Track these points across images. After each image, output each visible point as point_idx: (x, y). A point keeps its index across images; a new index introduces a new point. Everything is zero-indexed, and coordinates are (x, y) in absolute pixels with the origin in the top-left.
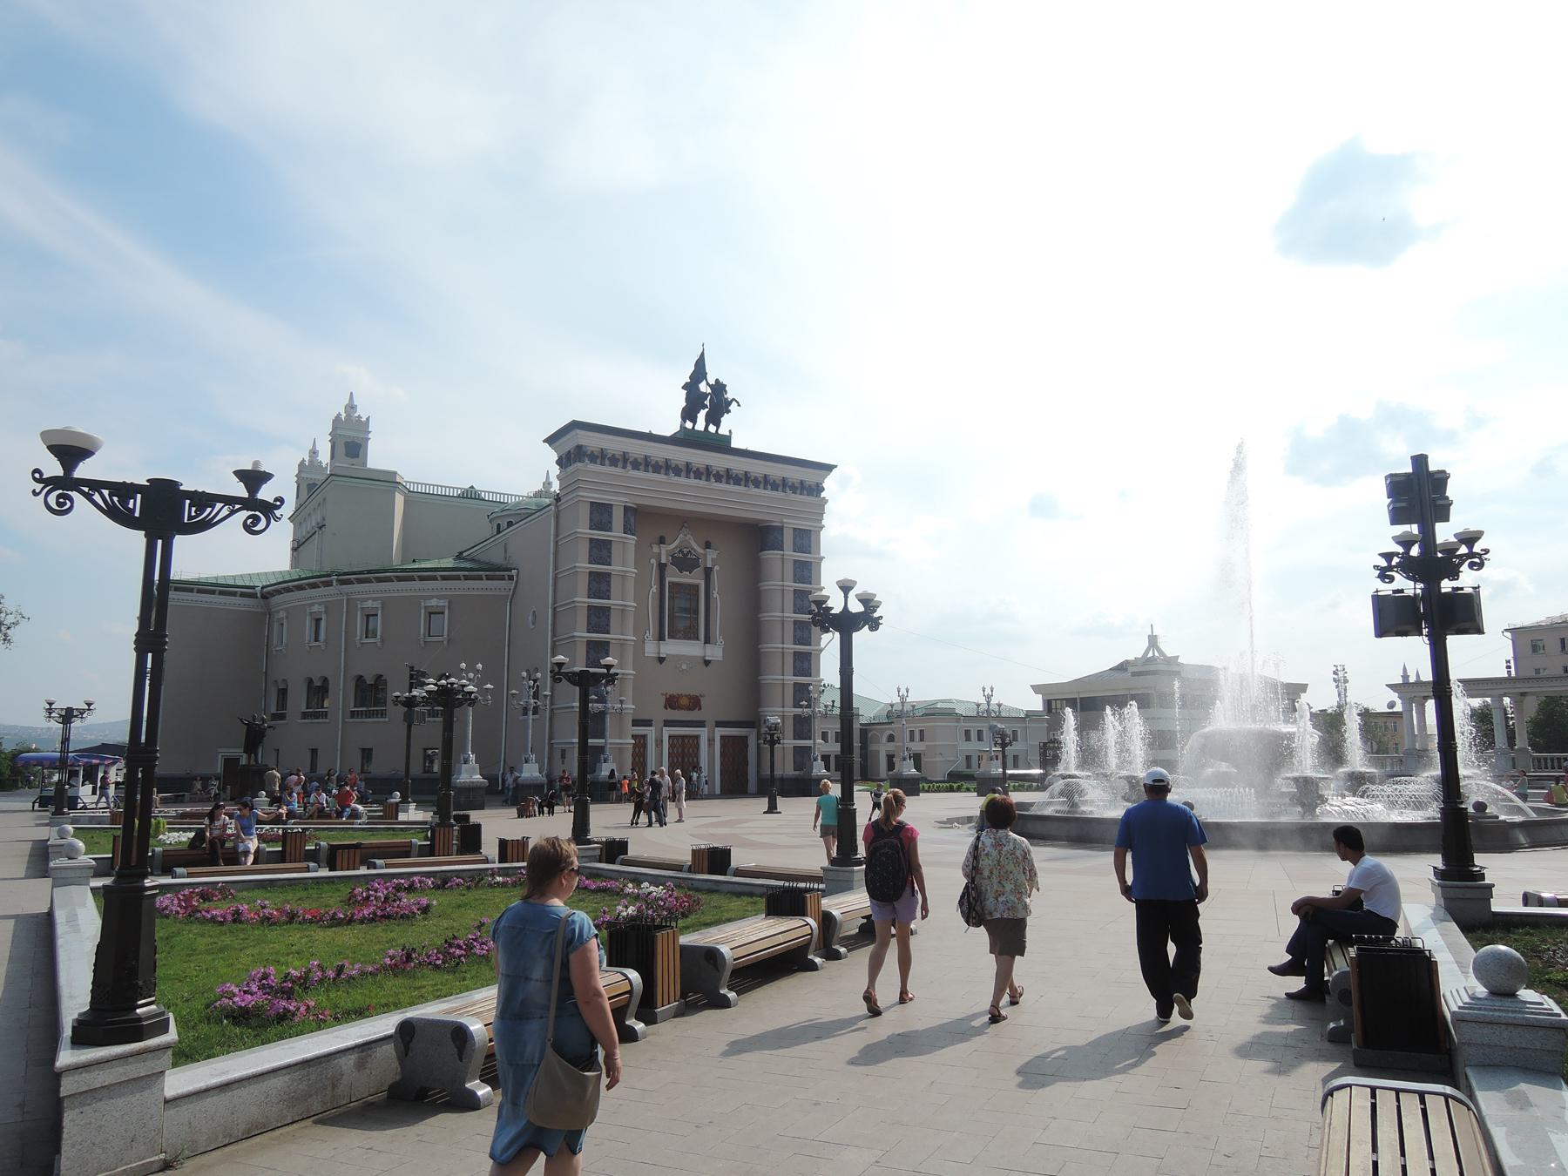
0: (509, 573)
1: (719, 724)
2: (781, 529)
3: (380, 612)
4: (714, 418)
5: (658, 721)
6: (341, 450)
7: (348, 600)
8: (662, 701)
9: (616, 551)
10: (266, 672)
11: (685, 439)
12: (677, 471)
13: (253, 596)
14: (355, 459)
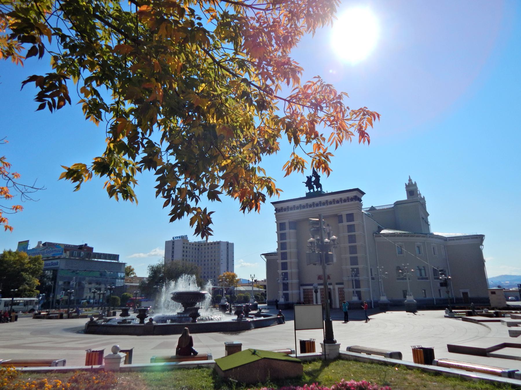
1: (337, 284)
2: (341, 215)
4: (319, 186)
5: (315, 284)
8: (317, 277)
9: (287, 236)
11: (309, 196)
12: (317, 205)
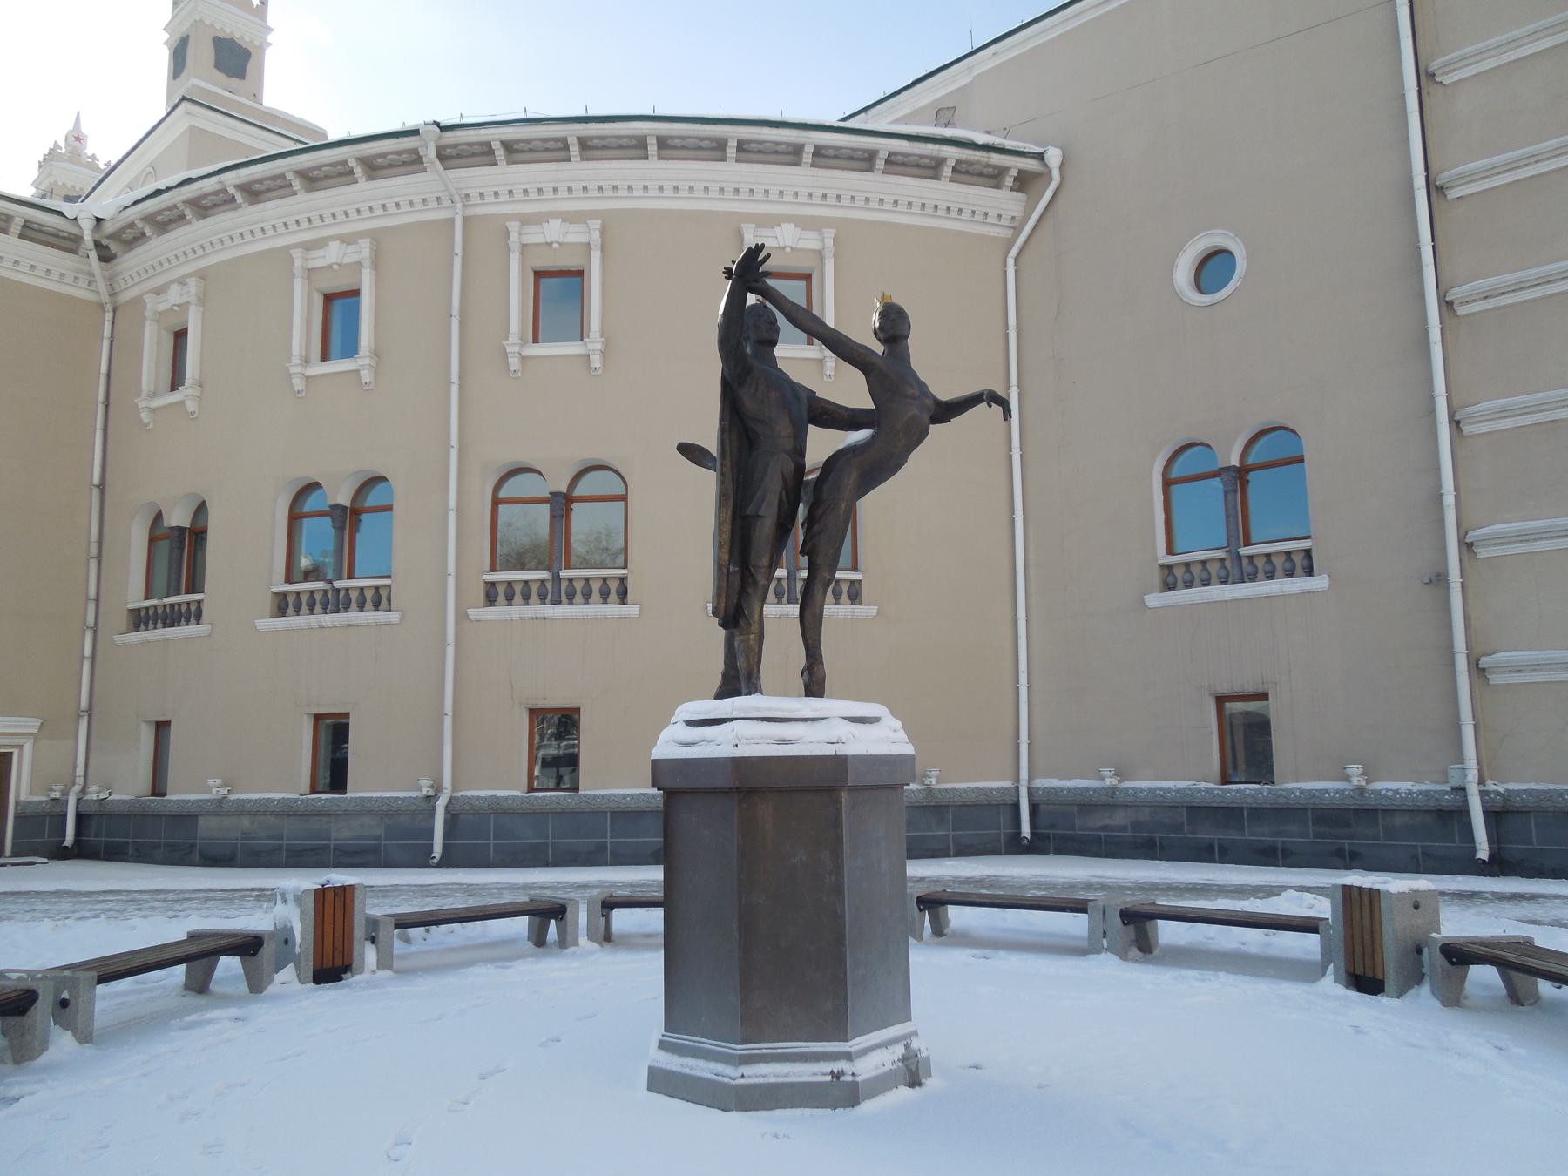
0: (1030, 165)
3: (596, 256)
6: (201, 54)
7: (465, 219)
10: (102, 486)
13: (68, 243)
14: (235, 80)
